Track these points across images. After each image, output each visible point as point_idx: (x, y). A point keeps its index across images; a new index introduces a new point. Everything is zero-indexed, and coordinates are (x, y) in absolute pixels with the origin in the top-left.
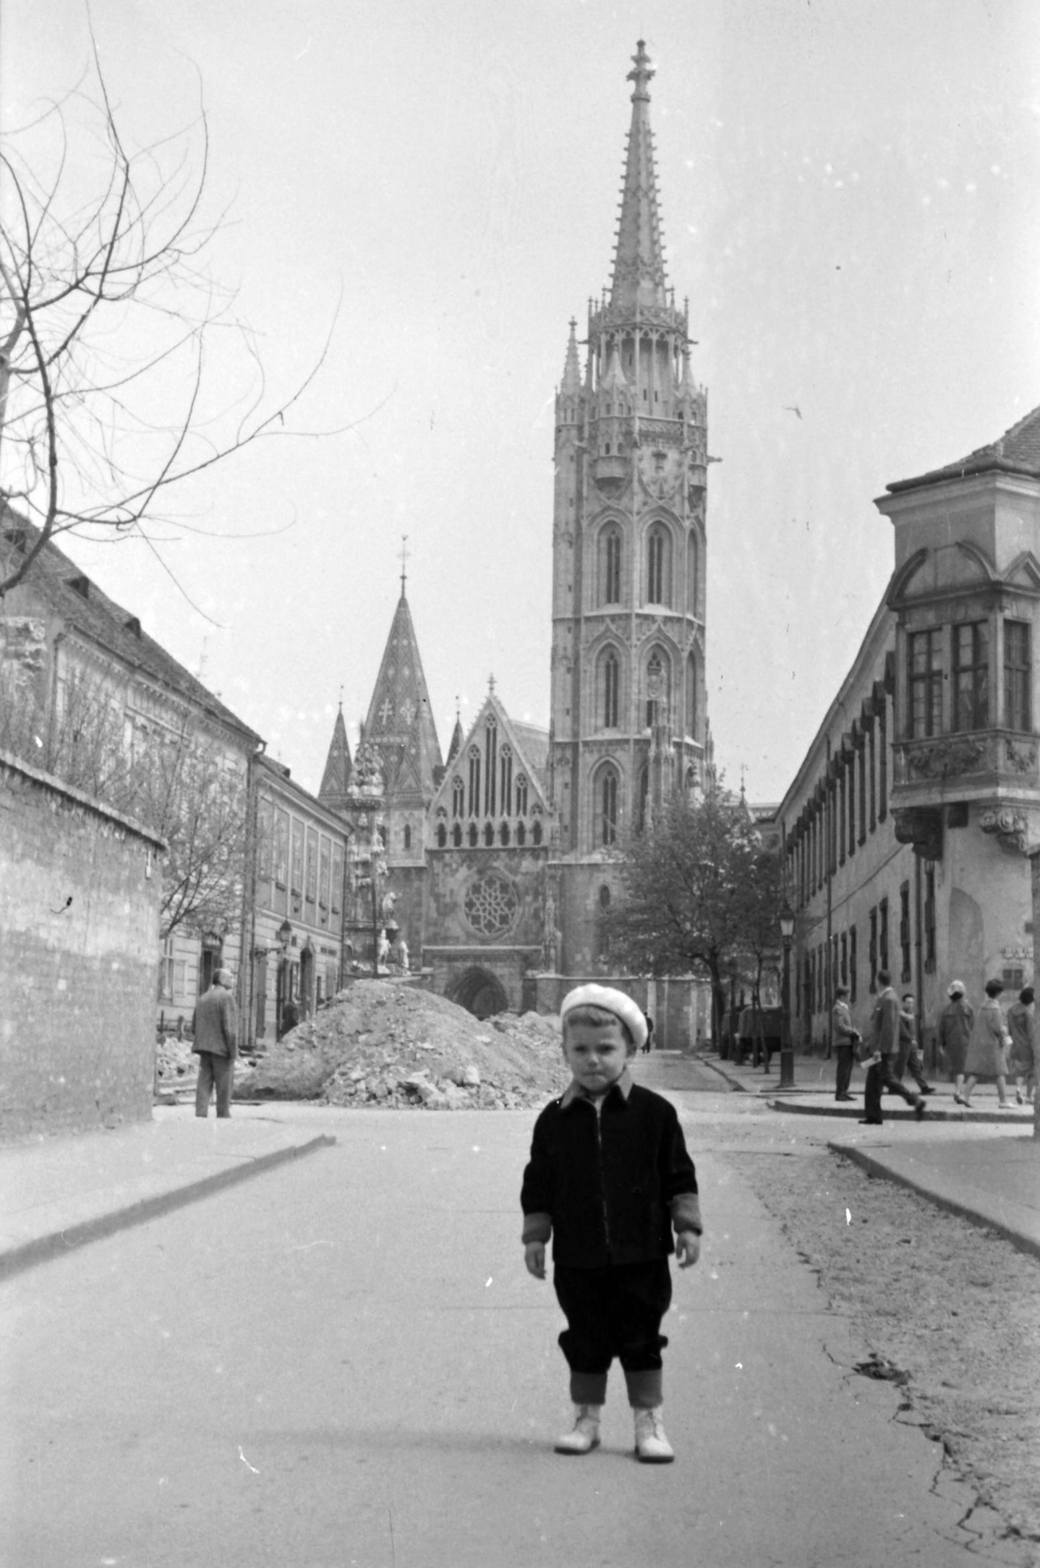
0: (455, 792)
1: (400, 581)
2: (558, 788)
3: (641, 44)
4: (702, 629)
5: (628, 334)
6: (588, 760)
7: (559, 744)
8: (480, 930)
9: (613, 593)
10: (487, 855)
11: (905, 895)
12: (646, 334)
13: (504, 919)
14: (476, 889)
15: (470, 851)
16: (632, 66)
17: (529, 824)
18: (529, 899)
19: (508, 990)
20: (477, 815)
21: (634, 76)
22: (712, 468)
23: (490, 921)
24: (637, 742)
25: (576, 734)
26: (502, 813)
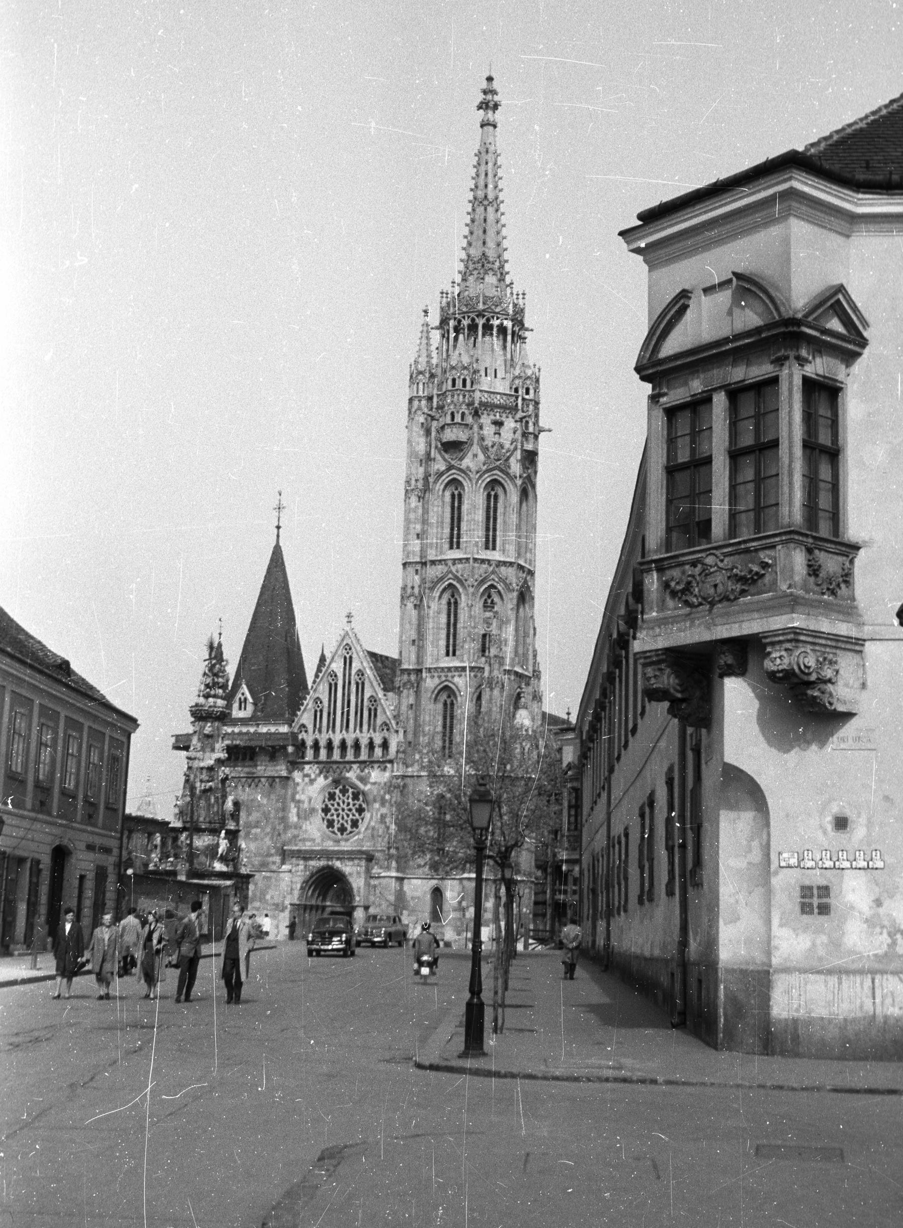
0: (316, 711)
1: (276, 531)
2: (404, 708)
3: (490, 79)
4: (531, 573)
5: (473, 320)
6: (430, 683)
7: (406, 670)
8: (333, 832)
9: (454, 542)
10: (341, 766)
11: (670, 782)
12: (488, 320)
13: (355, 824)
14: (332, 797)
15: (327, 763)
16: (481, 97)
17: (378, 741)
18: (377, 805)
19: (355, 886)
20: (334, 732)
21: (484, 106)
22: (542, 436)
23: (342, 825)
24: (472, 669)
25: (420, 659)
26: (355, 731)
